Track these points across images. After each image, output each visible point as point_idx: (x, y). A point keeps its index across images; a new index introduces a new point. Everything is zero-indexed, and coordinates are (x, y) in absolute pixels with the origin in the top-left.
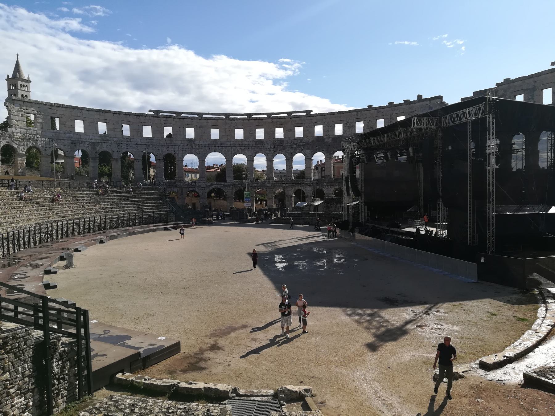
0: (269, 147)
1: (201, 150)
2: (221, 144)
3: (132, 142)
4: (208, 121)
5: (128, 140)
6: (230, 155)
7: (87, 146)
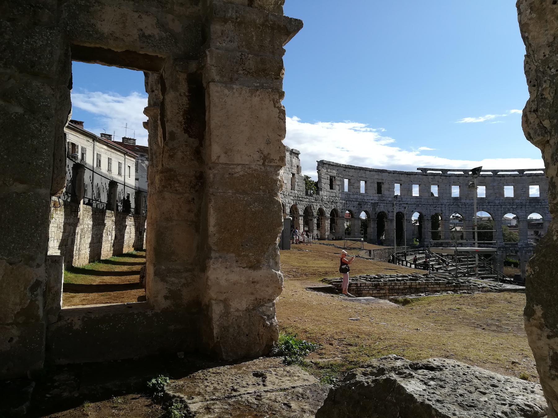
1: (468, 209)
2: (489, 203)
5: (400, 199)
6: (500, 214)
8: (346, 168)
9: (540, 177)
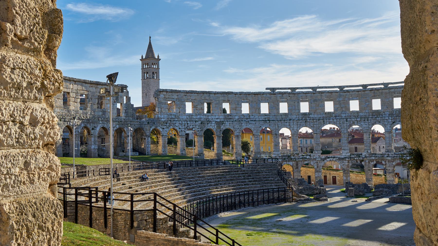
0: (387, 118)
1: (315, 123)
2: (335, 117)
3: (251, 119)
4: (323, 94)
5: (248, 117)
6: (346, 127)
8: (187, 93)
9: (380, 91)
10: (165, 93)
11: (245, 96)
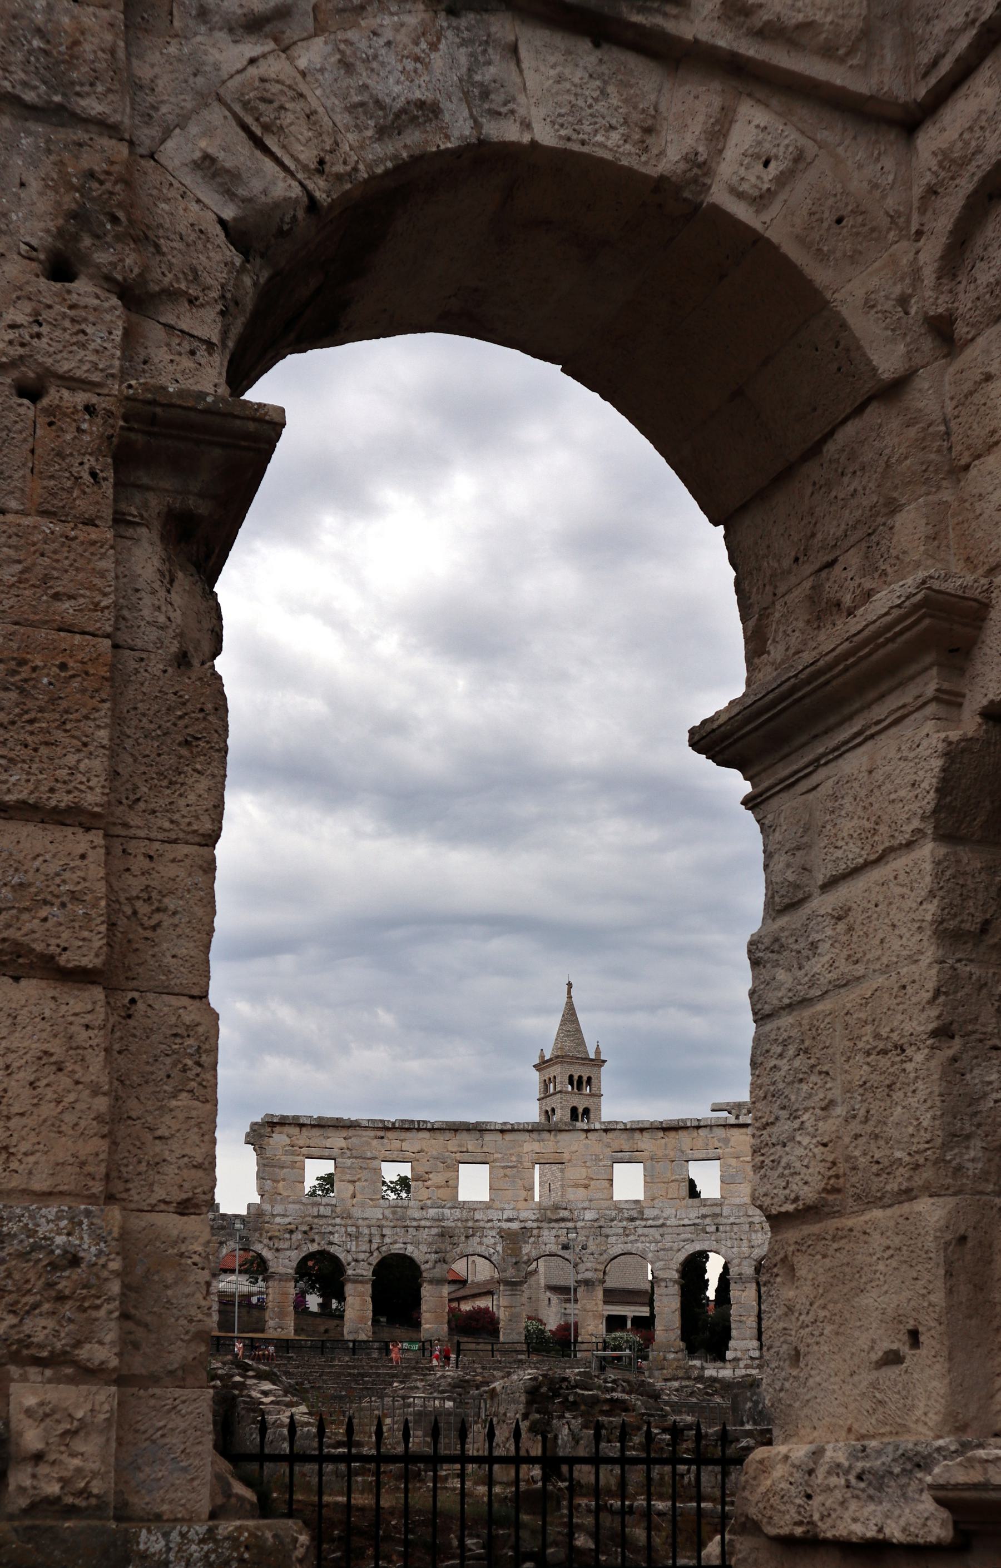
3: (647, 1219)
7: (492, 1241)
8: (387, 1129)
10: (296, 1130)
11: (625, 1135)
